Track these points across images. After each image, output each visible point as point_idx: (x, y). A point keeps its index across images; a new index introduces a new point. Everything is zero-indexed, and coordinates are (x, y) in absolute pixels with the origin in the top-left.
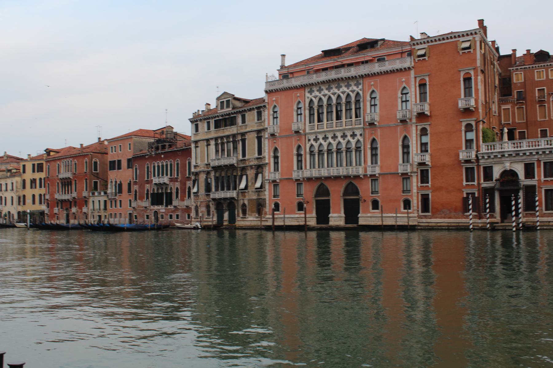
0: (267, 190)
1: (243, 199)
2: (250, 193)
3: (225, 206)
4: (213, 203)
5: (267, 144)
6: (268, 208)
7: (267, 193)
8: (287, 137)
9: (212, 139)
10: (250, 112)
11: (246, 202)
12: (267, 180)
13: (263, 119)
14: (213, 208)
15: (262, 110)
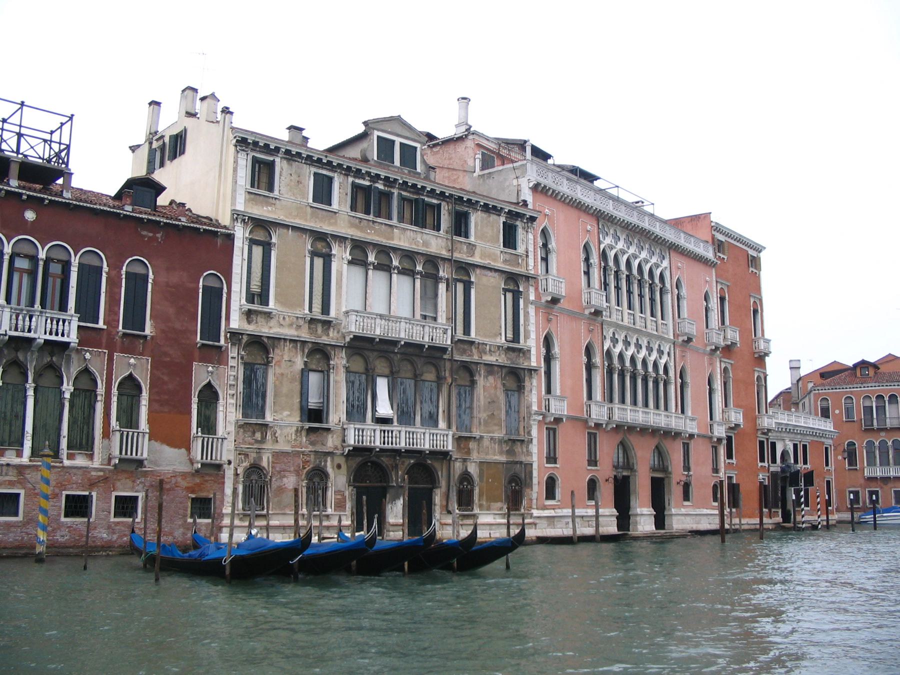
0: (535, 441)
1: (465, 460)
2: (486, 442)
3: (399, 477)
4: (342, 461)
5: (532, 320)
6: (537, 489)
7: (534, 448)
8: (574, 316)
9: (341, 239)
10: (484, 215)
11: (473, 469)
12: (537, 413)
13: (521, 250)
14: (338, 481)
15: (518, 223)
